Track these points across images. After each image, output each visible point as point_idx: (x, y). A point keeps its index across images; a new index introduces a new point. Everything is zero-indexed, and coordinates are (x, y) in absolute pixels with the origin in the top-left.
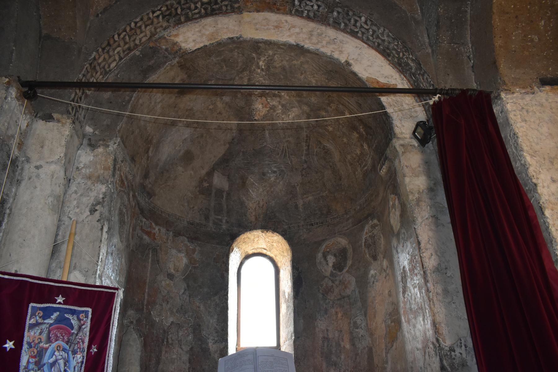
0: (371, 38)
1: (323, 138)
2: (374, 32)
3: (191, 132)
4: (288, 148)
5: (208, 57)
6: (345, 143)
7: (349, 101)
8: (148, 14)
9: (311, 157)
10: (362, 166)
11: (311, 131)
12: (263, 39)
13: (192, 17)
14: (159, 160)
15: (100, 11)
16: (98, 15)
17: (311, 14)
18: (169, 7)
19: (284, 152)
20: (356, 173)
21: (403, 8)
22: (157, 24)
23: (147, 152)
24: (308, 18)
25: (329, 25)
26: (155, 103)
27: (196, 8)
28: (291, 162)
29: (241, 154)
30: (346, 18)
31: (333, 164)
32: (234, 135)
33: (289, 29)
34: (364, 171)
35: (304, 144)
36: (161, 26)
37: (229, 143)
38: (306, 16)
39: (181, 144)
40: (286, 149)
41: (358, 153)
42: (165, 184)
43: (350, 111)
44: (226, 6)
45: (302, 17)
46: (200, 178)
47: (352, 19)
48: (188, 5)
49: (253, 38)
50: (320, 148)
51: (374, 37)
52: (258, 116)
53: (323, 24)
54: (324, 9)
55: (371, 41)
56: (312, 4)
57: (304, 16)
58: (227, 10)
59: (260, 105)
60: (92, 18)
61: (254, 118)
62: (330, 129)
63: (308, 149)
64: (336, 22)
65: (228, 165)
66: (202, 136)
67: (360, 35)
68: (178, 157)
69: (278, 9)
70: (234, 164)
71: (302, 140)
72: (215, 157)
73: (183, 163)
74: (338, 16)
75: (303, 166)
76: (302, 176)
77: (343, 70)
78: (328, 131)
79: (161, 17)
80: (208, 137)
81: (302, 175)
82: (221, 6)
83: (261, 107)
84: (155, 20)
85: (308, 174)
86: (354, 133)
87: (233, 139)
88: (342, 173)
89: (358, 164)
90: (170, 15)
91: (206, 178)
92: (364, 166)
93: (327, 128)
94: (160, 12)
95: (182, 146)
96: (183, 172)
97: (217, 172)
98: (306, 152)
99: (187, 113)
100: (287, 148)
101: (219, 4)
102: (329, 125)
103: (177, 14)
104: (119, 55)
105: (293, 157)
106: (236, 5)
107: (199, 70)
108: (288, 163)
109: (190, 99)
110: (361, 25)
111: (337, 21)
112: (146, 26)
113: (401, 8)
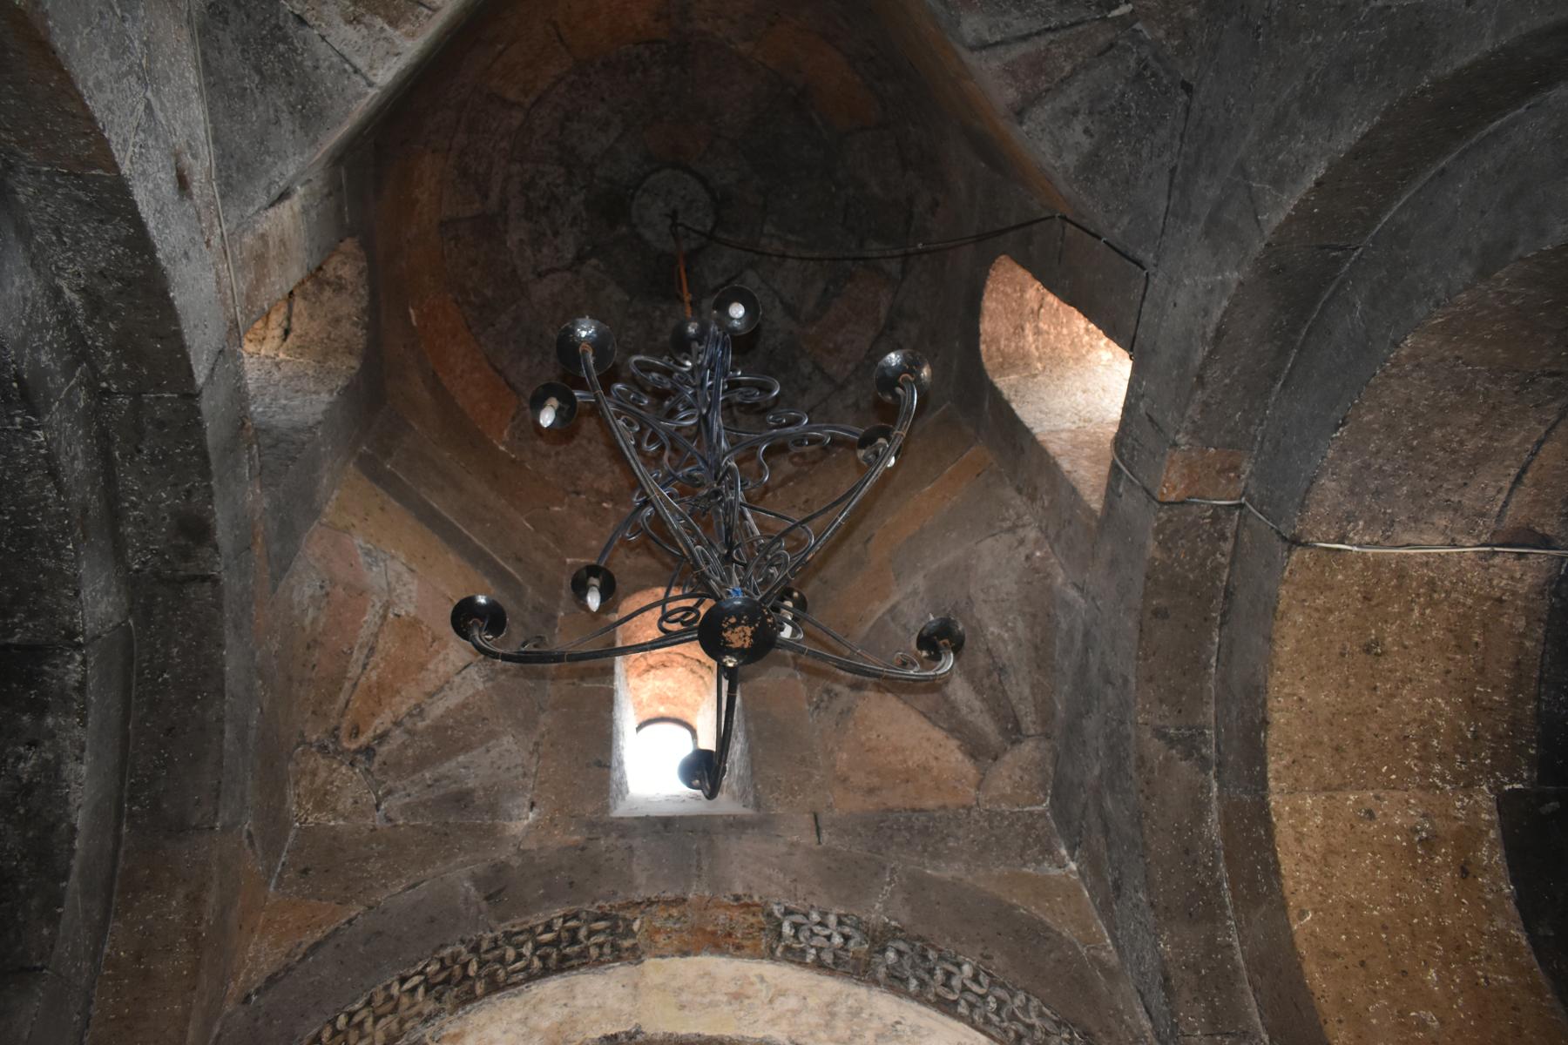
0: (995, 1019)
2: (1001, 1003)
8: (388, 987)
12: (699, 1036)
13: (505, 980)
15: (257, 986)
16: (247, 998)
17: (828, 958)
18: (448, 962)
21: (1064, 934)
22: (409, 1008)
24: (819, 965)
25: (877, 983)
27: (520, 957)
30: (922, 965)
33: (771, 1001)
36: (419, 1014)
38: (813, 961)
44: (600, 946)
45: (802, 964)
47: (938, 968)
48: (497, 952)
49: (671, 1035)
51: (1004, 1016)
53: (859, 980)
54: (861, 944)
55: (996, 1026)
56: (827, 932)
57: (808, 960)
58: (601, 955)
60: (229, 1007)
64: (896, 977)
67: (963, 1009)
69: (739, 947)
74: (899, 961)
79: (421, 990)
82: (587, 948)
84: (405, 1001)
90: (446, 981)
94: (422, 978)
101: (581, 943)
103: (466, 977)
106: (627, 943)
110: (964, 985)
111: (897, 974)
112: (376, 1021)
113: (1059, 934)
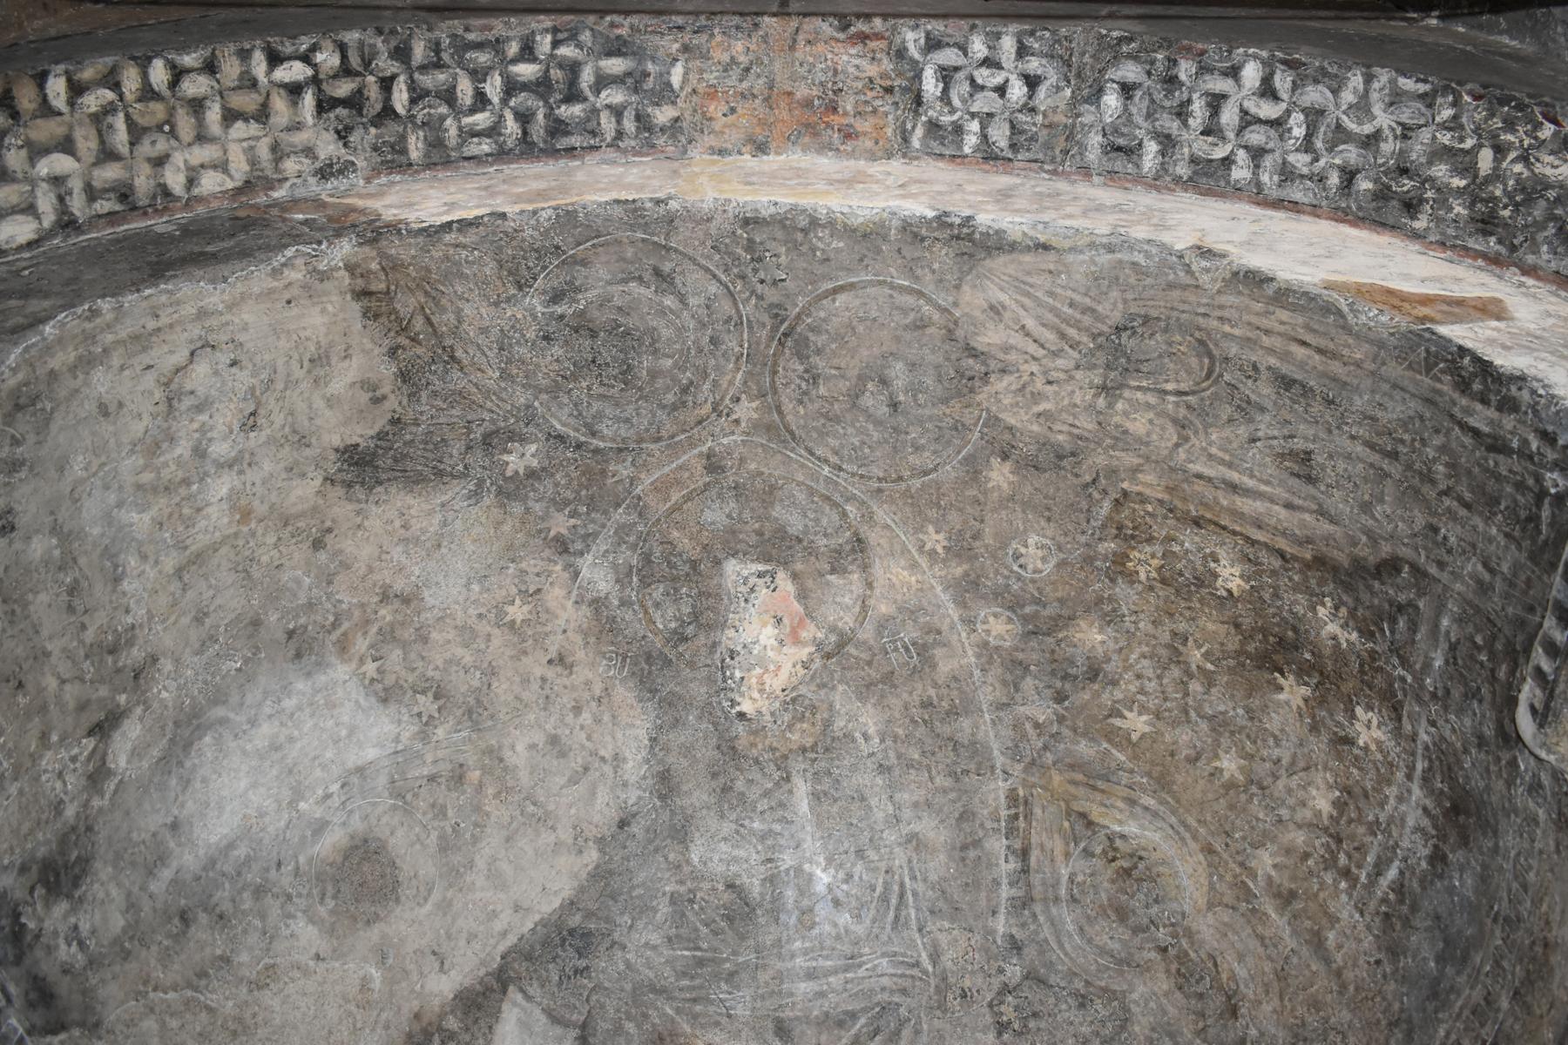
0: (1300, 161)
1: (1103, 791)
2: (1314, 115)
3: (397, 740)
4: (914, 878)
5: (513, 291)
6: (1231, 785)
7: (1234, 476)
8: (245, 55)
9: (1041, 919)
10: (1363, 878)
11: (1033, 763)
13: (460, 146)
14: (175, 826)
17: (1000, 135)
18: (355, 61)
19: (894, 901)
20: (1331, 936)
22: (289, 129)
23: (103, 728)
24: (988, 155)
25: (1085, 171)
26: (199, 452)
27: (481, 101)
28: (930, 956)
29: (664, 909)
30: (1167, 104)
31: (1175, 936)
32: (632, 796)
34: (1384, 901)
35: (997, 845)
36: (309, 152)
37: (601, 842)
38: (977, 149)
39: (335, 788)
40: (902, 885)
41: (1318, 814)
42: (189, 993)
43: (1247, 539)
44: (617, 112)
45: (957, 158)
46: (417, 1016)
47: (1195, 96)
48: (442, 77)
50: (1087, 853)
51: (1319, 144)
52: (756, 695)
53: (1054, 172)
54: (1058, 89)
55: (1302, 176)
56: (998, 79)
57: (967, 150)
58: (620, 134)
59: (764, 625)
61: (733, 703)
62: (1137, 723)
63: (1025, 871)
64: (1119, 149)
65: (587, 968)
66: (458, 777)
67: (1241, 173)
68: (302, 859)
69: (849, 135)
70: (622, 967)
71: (989, 824)
72: (517, 908)
73: (331, 903)
74: (1126, 109)
75: (1001, 971)
76: (1000, 1034)
77: (1185, 287)
78: (1121, 739)
79: (309, 99)
80: (490, 791)
81: (1002, 1027)
82: (595, 111)
83: (773, 642)
84: (279, 104)
85: (1035, 1015)
86: (1280, 689)
87: (623, 824)
88: (1242, 973)
89: (1329, 878)
90: (355, 102)
91: (452, 1023)
92: (1379, 870)
93: (1117, 722)
94: (310, 72)
95: (336, 801)
96: (318, 957)
97: (519, 997)
98: (1014, 892)
99: (386, 614)
100: (907, 880)
101: (585, 99)
102: (1130, 703)
103: (388, 112)
104: (61, 199)
105: (946, 925)
106: (663, 115)
107: (459, 354)
108: (917, 964)
109: (405, 527)
110: (1244, 112)
111: (1121, 142)
112: (230, 116)
